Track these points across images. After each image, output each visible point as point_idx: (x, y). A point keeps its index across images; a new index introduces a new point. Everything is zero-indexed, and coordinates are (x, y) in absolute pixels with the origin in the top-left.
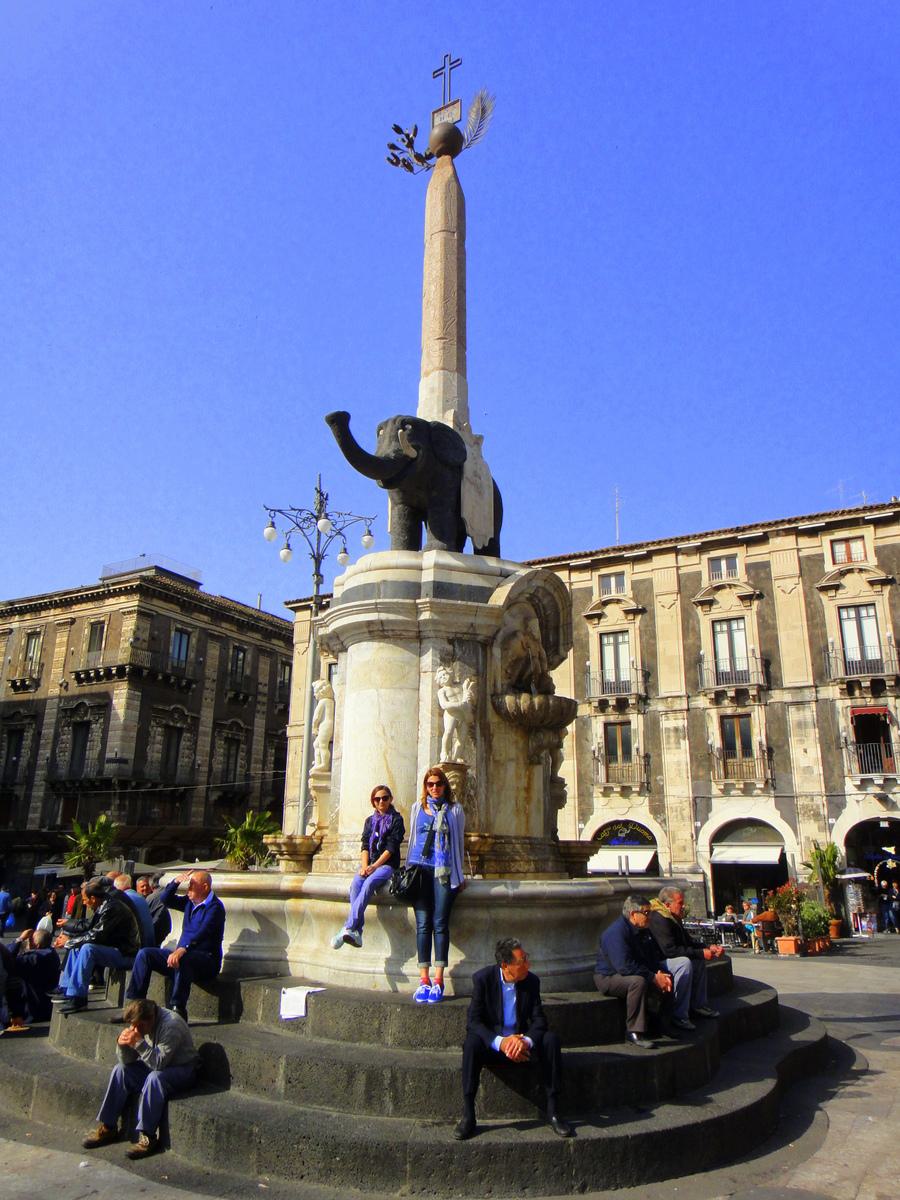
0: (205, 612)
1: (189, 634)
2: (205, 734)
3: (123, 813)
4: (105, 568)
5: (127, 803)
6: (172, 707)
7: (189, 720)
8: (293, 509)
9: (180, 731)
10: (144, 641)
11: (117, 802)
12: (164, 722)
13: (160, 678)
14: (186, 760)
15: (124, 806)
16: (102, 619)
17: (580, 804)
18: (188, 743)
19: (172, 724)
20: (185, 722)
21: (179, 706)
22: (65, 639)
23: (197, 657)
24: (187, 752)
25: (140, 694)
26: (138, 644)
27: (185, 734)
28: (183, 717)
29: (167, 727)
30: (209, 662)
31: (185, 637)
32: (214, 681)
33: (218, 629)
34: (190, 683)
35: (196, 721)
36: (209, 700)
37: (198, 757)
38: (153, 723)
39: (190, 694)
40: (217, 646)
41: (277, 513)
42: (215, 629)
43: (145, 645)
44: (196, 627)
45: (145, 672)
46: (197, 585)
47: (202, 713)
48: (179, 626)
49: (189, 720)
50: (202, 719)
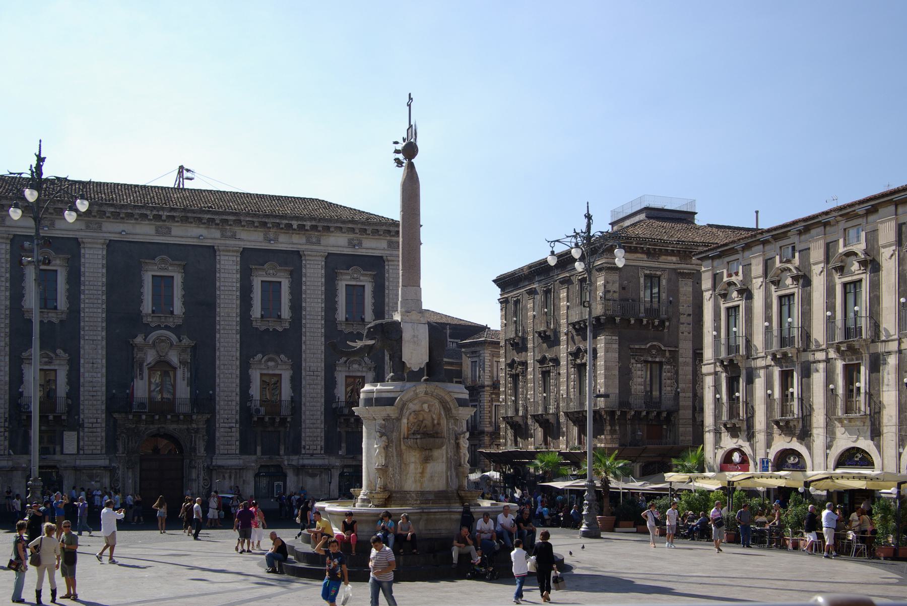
0: (672, 253)
1: (659, 277)
2: (686, 364)
3: (614, 436)
4: (613, 212)
5: (617, 428)
6: (648, 345)
7: (667, 354)
8: (568, 237)
9: (661, 364)
10: (614, 292)
11: (609, 428)
12: (642, 358)
13: (633, 322)
14: (669, 389)
15: (615, 430)
16: (585, 276)
17: (900, 430)
18: (669, 374)
19: (650, 359)
20: (664, 355)
21: (654, 343)
22: (565, 294)
23: (668, 296)
24: (669, 381)
25: (617, 338)
26: (609, 296)
27: (664, 367)
28: (661, 352)
29: (646, 362)
30: (682, 299)
31: (655, 280)
32: (689, 315)
33: (689, 266)
34: (662, 322)
35: (674, 355)
36: (686, 334)
37: (680, 386)
38: (633, 361)
39: (666, 330)
40: (690, 282)
41: (556, 243)
42: (684, 267)
43: (616, 296)
44: (664, 270)
45: (618, 319)
46: (685, 217)
47: (680, 346)
48: (648, 272)
49: (667, 354)
50: (680, 351)
